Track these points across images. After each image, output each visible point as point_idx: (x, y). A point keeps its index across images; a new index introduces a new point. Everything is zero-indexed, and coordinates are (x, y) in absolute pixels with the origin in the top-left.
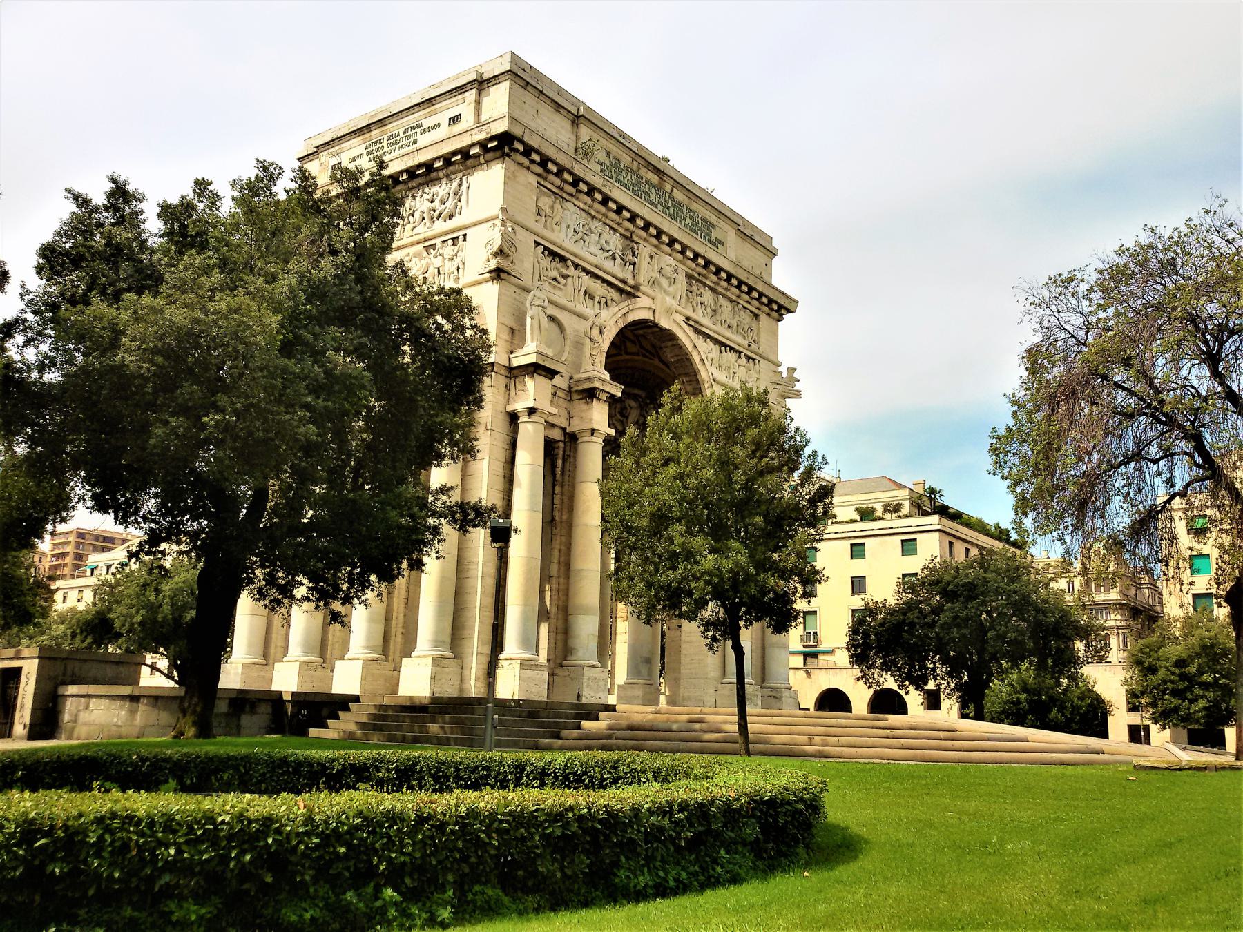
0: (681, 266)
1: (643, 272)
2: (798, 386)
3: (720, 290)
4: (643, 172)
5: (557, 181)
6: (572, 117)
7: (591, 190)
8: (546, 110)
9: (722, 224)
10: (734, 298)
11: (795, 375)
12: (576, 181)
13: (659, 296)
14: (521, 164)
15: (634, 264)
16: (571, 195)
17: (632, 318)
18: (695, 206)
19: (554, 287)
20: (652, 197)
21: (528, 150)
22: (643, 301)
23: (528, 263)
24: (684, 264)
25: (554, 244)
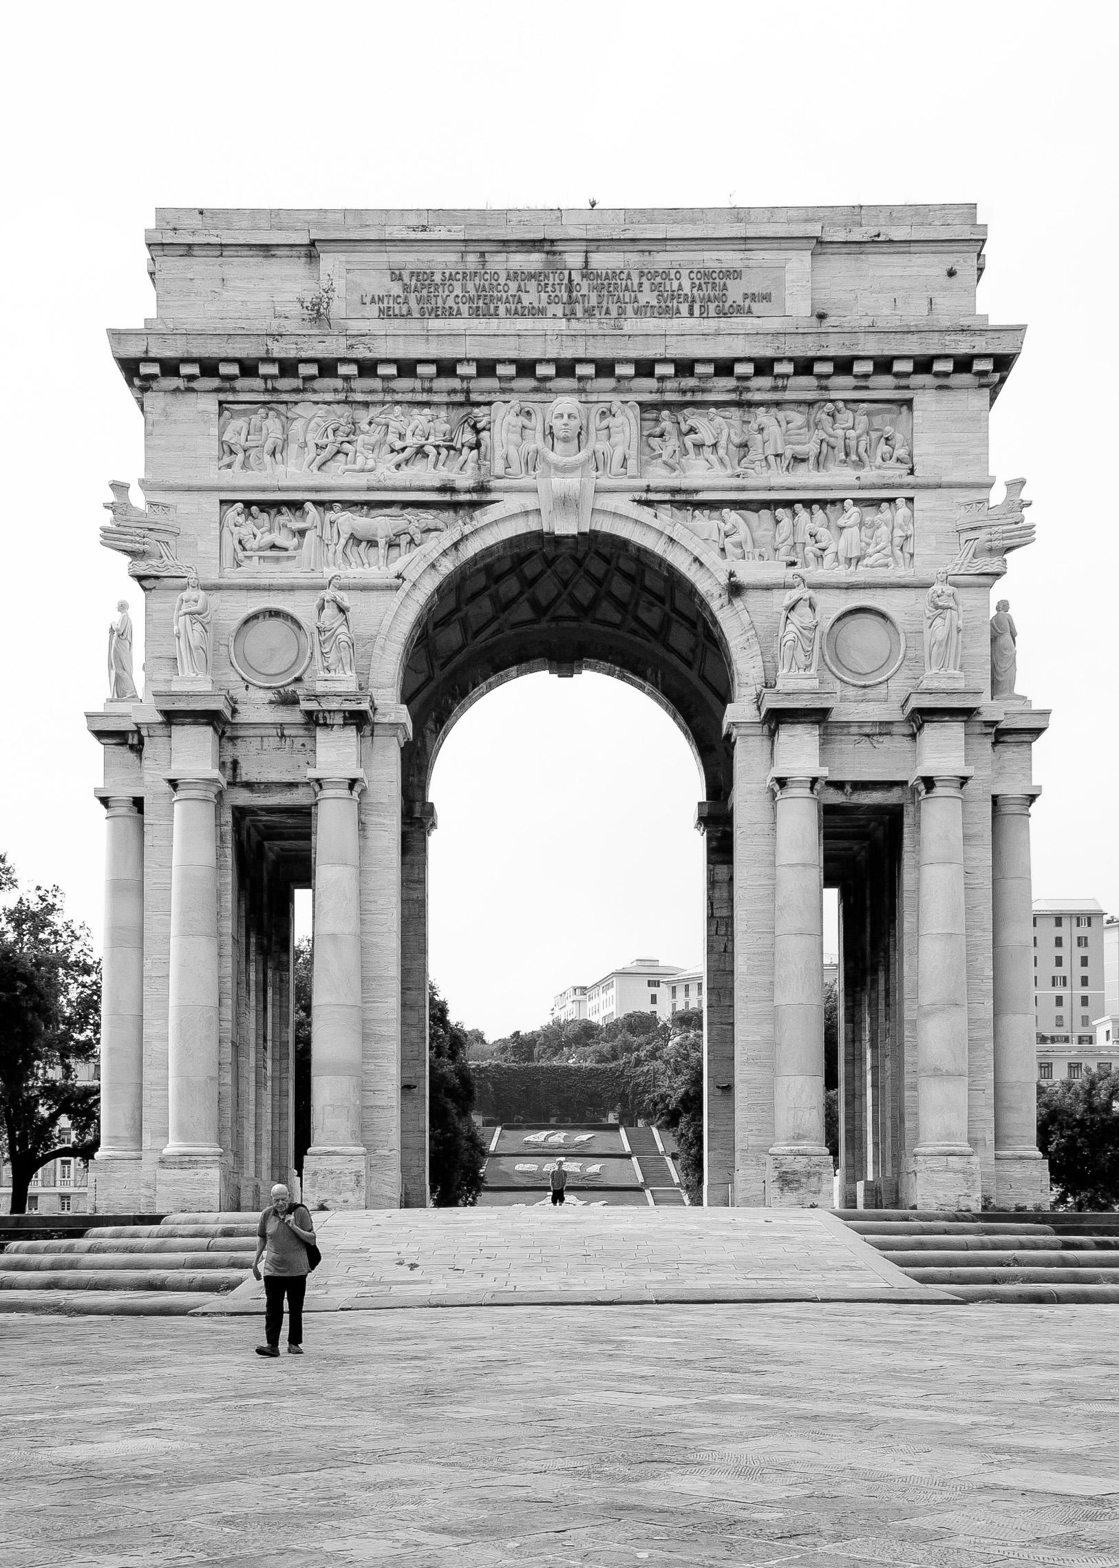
0: (616, 399)
1: (499, 453)
2: (1029, 515)
3: (757, 397)
4: (499, 262)
5: (257, 383)
6: (303, 251)
7: (327, 368)
8: (242, 270)
9: (761, 256)
10: (810, 396)
11: (1025, 495)
12: (288, 367)
13: (541, 484)
14: (177, 390)
15: (478, 445)
16: (296, 391)
17: (472, 549)
18: (662, 260)
19: (277, 559)
20: (526, 300)
21: (170, 367)
22: (510, 504)
23: (203, 540)
24: (630, 391)
25: (263, 490)
